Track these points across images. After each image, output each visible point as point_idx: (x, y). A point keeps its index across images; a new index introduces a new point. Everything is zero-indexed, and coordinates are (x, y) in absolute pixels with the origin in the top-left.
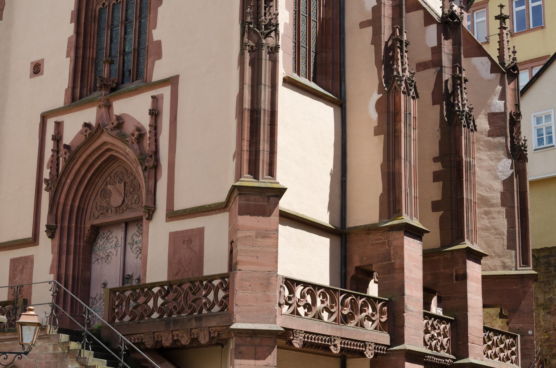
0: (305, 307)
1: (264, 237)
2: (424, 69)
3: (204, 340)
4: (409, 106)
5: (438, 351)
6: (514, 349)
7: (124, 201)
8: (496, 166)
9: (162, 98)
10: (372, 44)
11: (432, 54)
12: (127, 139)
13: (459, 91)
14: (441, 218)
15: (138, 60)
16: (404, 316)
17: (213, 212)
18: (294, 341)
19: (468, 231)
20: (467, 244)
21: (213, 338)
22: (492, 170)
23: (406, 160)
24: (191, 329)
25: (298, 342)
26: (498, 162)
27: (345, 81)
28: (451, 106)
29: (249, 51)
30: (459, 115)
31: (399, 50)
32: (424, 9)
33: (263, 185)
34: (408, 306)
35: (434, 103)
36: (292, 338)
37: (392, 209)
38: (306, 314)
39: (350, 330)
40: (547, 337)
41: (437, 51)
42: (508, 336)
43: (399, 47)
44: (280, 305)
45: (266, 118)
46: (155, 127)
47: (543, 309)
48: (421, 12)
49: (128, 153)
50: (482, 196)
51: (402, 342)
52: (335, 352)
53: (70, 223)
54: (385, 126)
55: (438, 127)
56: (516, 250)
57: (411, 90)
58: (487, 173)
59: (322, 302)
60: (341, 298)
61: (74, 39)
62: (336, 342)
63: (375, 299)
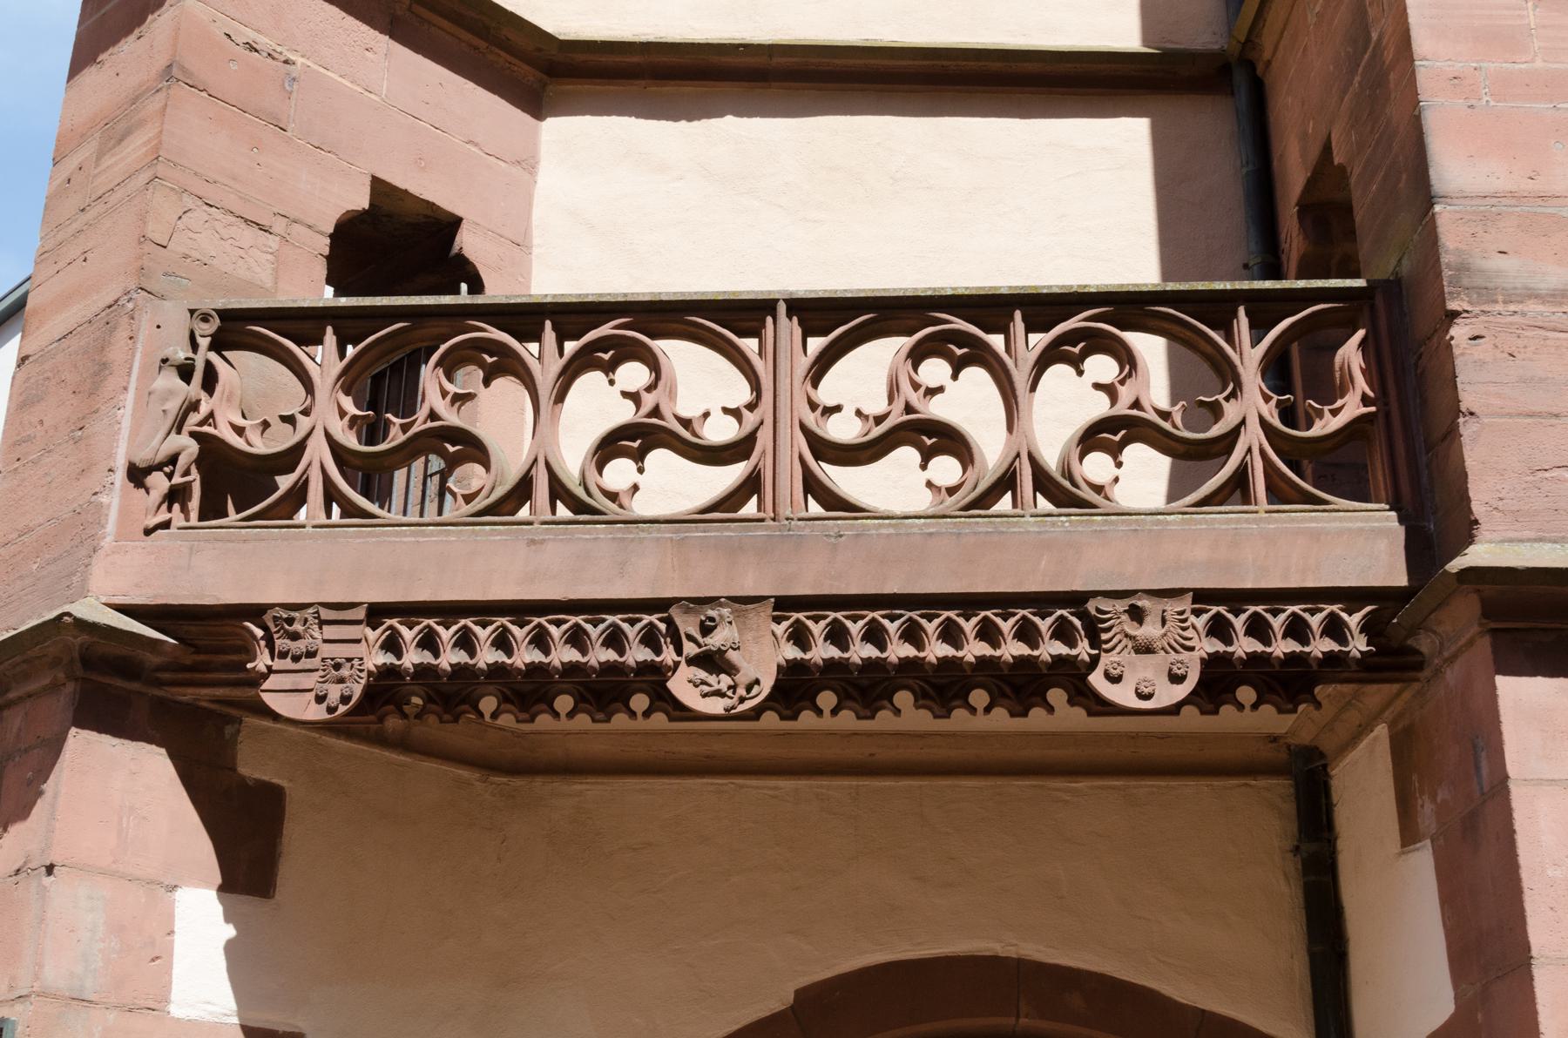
25: (309, 681)
52: (716, 706)
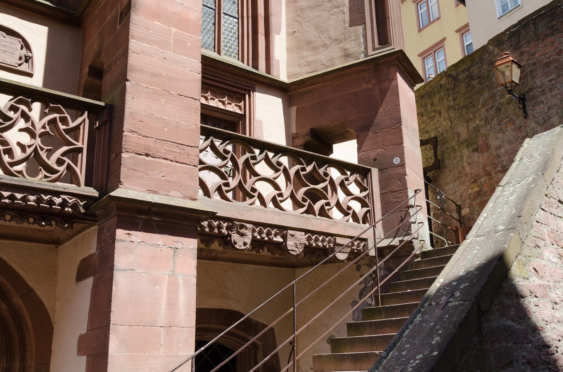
40: (476, 189)
56: (365, 23)
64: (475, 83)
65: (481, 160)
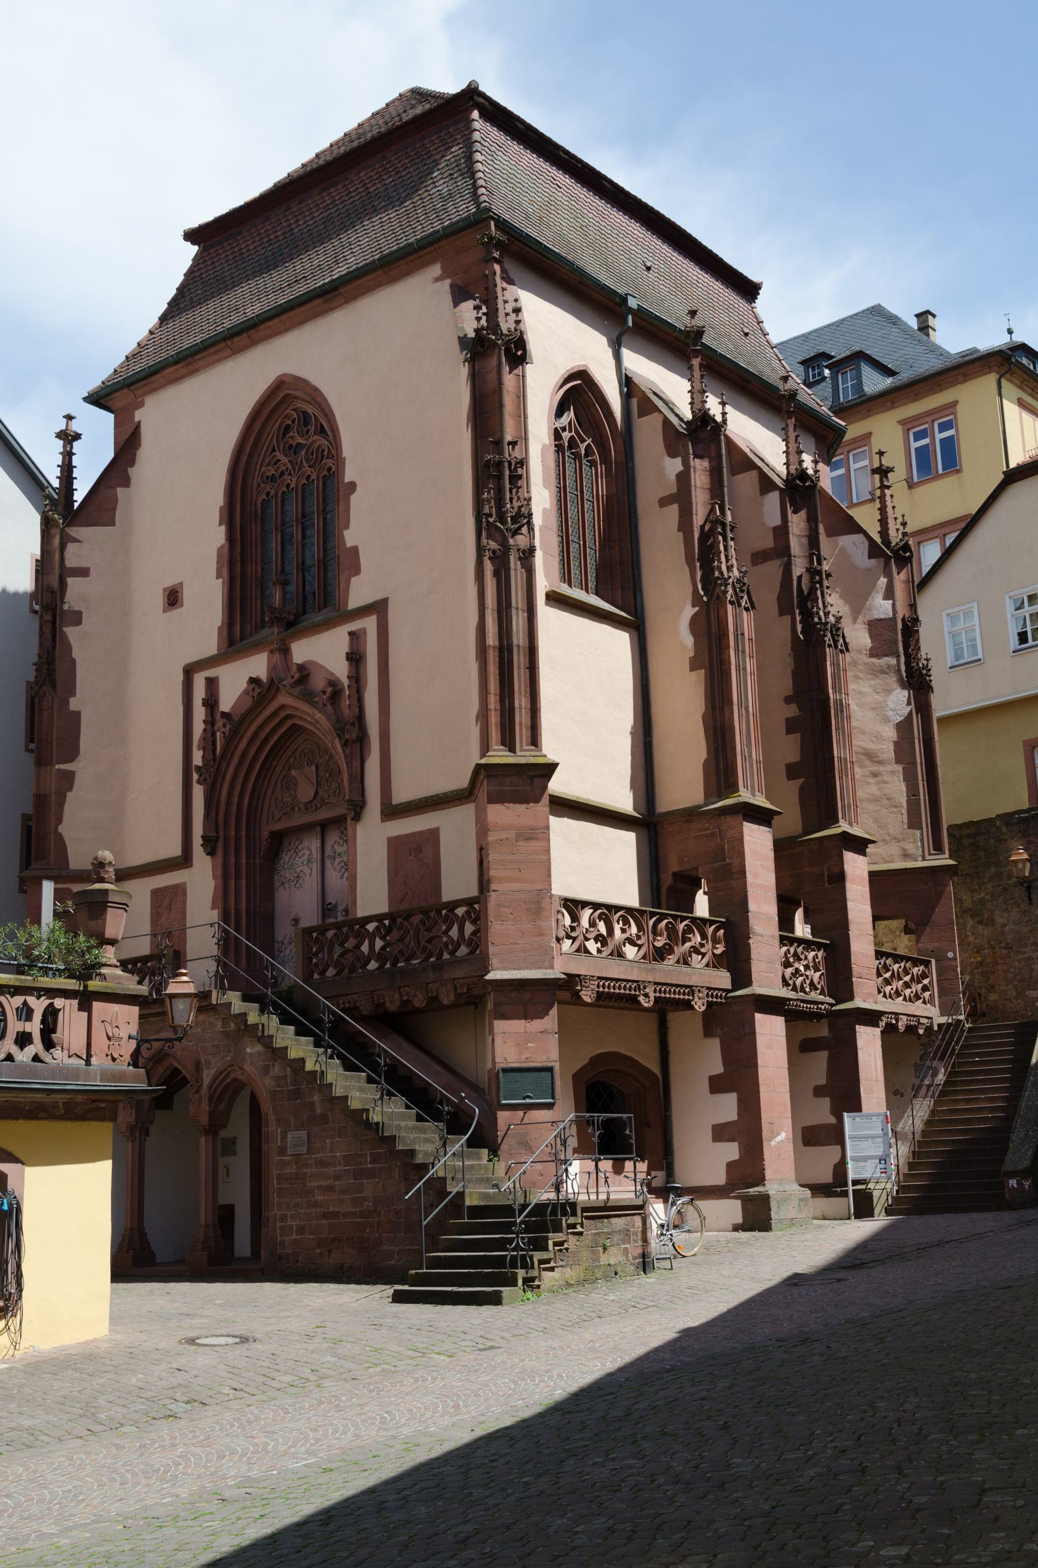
0: (596, 940)
1: (528, 839)
2: (764, 561)
3: (447, 998)
4: (741, 623)
5: (806, 993)
6: (926, 981)
7: (316, 794)
8: (885, 701)
9: (365, 633)
10: (679, 530)
11: (775, 537)
12: (316, 699)
13: (819, 592)
14: (802, 790)
15: (325, 577)
16: (749, 944)
17: (451, 804)
18: (582, 993)
19: (843, 806)
20: (843, 826)
21: (461, 994)
22: (878, 709)
23: (740, 705)
24: (427, 984)
26: (887, 695)
27: (641, 590)
28: (808, 615)
29: (490, 558)
30: (820, 630)
31: (720, 538)
32: (759, 468)
33: (523, 761)
34: (755, 927)
35: (782, 613)
36: (579, 988)
37: (723, 782)
38: (599, 951)
39: (669, 971)
40: (979, 959)
41: (782, 532)
42: (916, 962)
43: (720, 533)
44: (558, 940)
45: (522, 659)
46: (357, 678)
47: (972, 916)
48: (754, 473)
49: (317, 720)
50: (866, 749)
51: (749, 983)
52: (646, 1005)
53: (237, 830)
54: (706, 655)
55: (788, 650)
57: (742, 598)
58: (871, 714)
59: (623, 931)
60: (651, 922)
61: (226, 550)
62: (647, 990)
63: (704, 921)
64: (981, 854)
65: (986, 933)
